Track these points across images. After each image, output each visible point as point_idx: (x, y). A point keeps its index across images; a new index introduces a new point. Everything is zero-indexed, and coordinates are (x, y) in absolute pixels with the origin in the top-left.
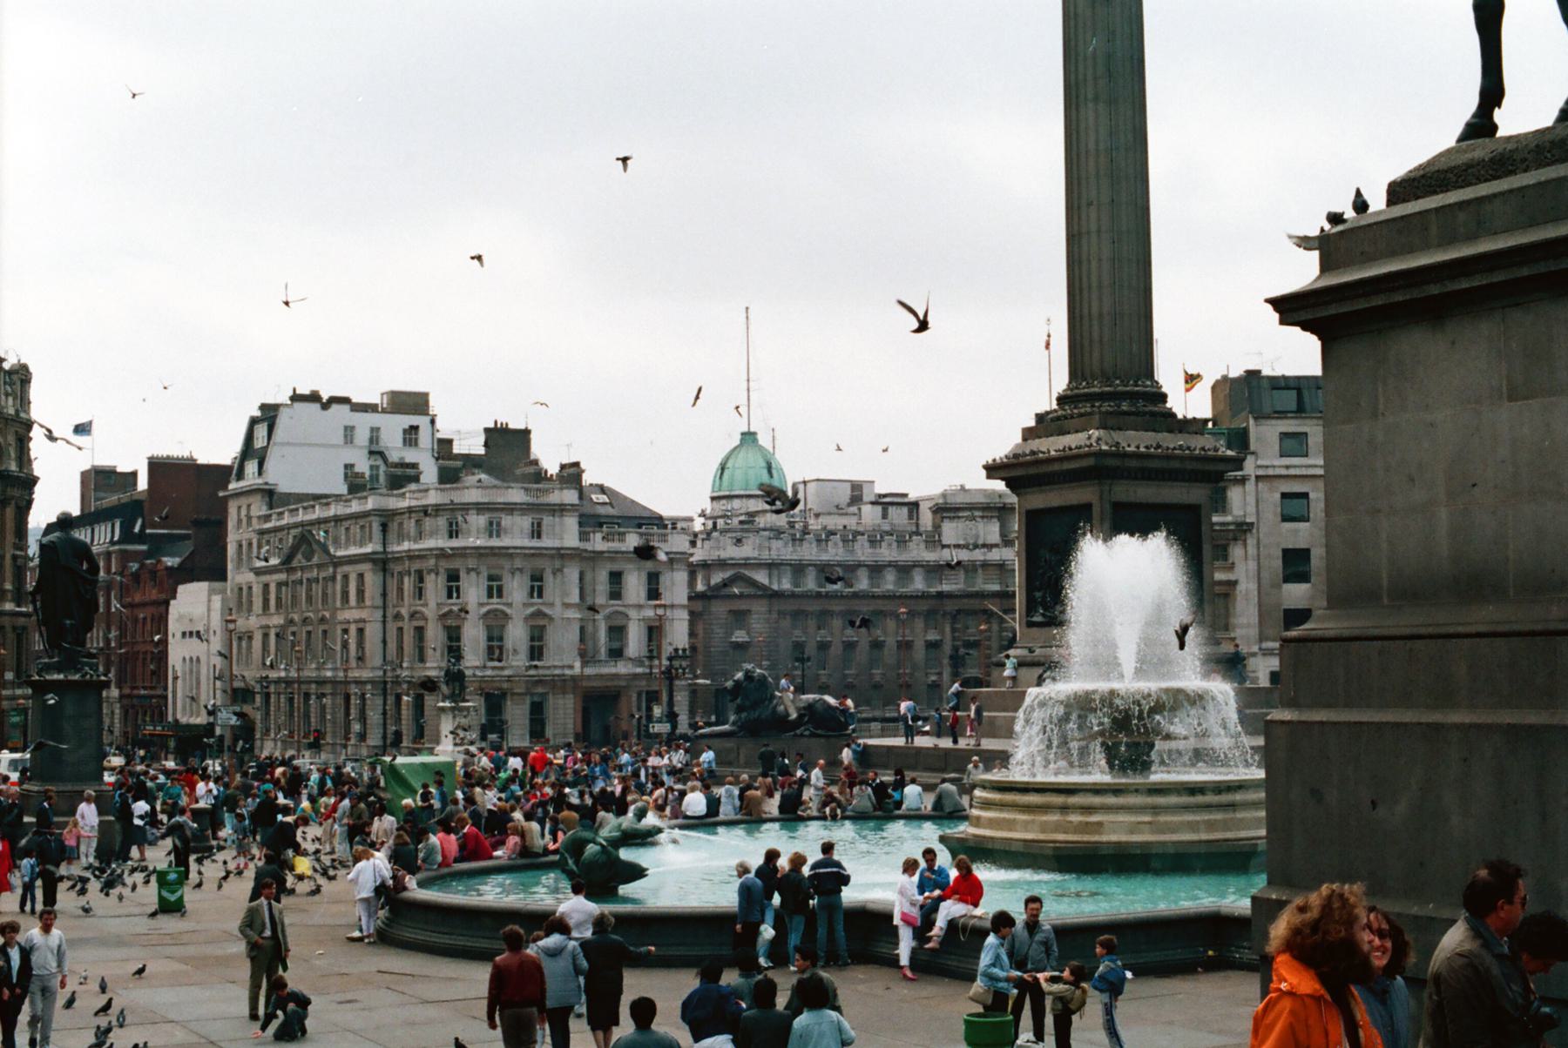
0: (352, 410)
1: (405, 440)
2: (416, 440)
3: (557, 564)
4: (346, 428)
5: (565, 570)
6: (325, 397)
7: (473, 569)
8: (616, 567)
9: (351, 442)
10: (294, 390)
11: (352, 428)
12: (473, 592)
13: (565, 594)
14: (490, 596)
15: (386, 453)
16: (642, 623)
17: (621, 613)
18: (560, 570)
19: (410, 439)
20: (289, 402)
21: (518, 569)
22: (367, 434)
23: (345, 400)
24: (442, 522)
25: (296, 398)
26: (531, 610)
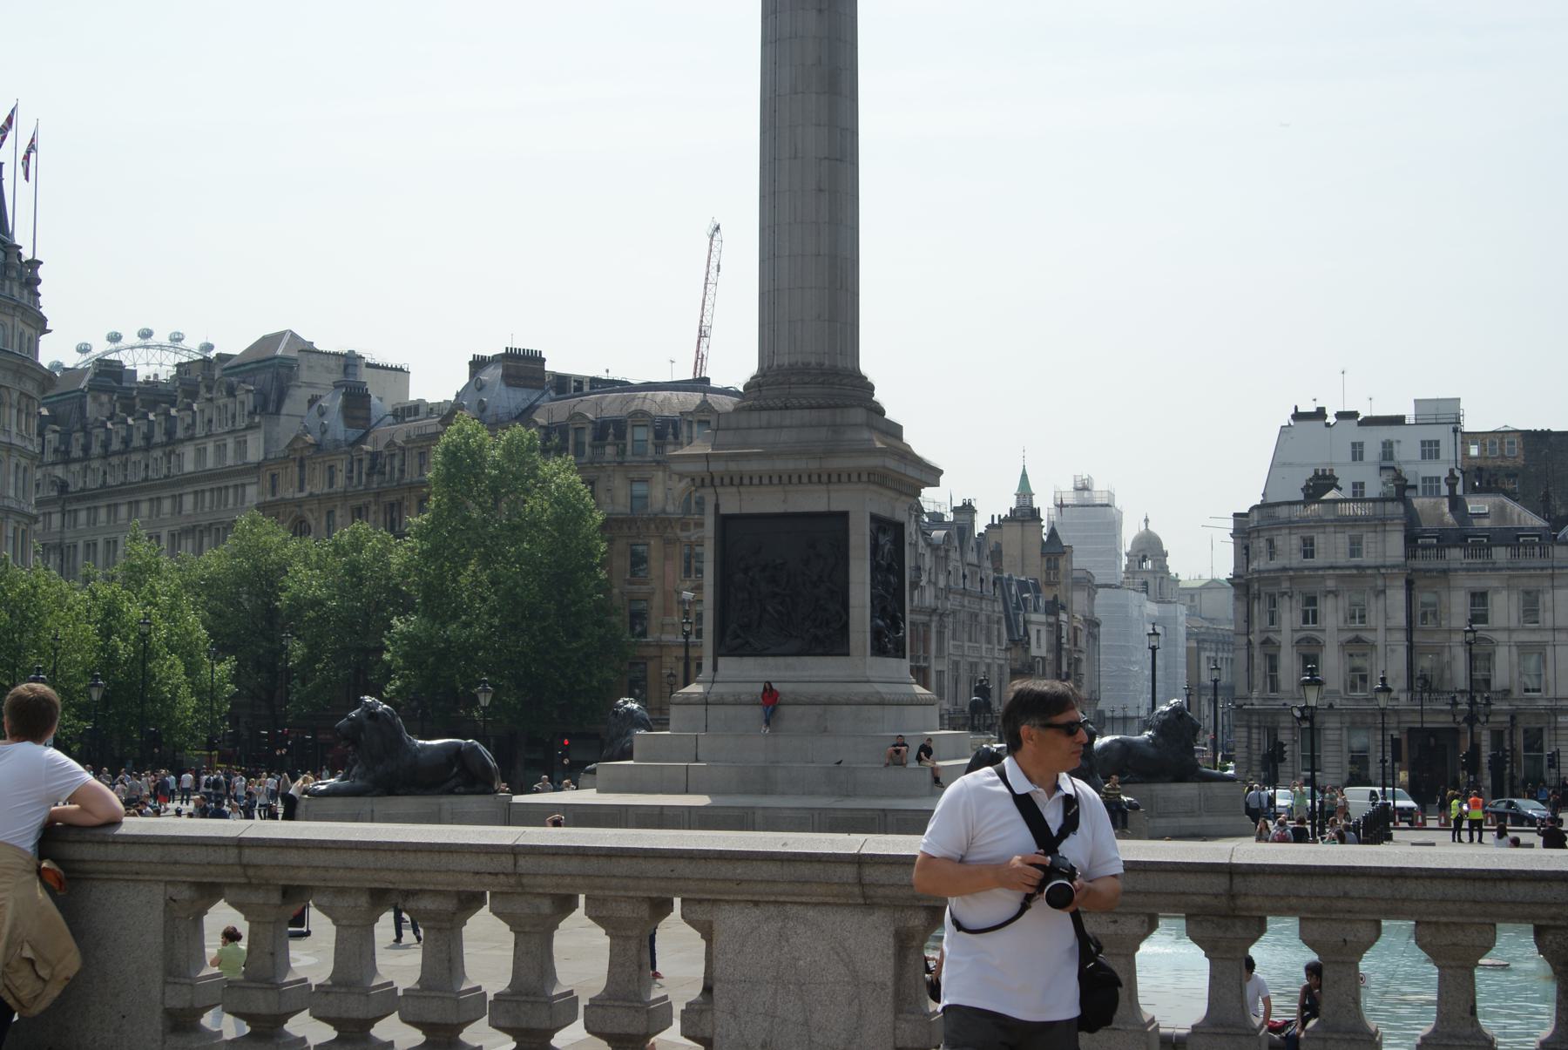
0: (1361, 424)
1: (1423, 452)
2: (1437, 452)
3: (1380, 582)
4: (1354, 445)
5: (1387, 591)
7: (1285, 593)
8: (1478, 584)
9: (1361, 459)
10: (1296, 408)
11: (1361, 444)
12: (1290, 617)
13: (1387, 617)
14: (1306, 621)
15: (1396, 467)
16: (1514, 650)
17: (1485, 639)
18: (1384, 592)
19: (1430, 451)
21: (1330, 592)
22: (1380, 449)
23: (1355, 415)
24: (1262, 543)
25: (1298, 416)
26: (1351, 635)
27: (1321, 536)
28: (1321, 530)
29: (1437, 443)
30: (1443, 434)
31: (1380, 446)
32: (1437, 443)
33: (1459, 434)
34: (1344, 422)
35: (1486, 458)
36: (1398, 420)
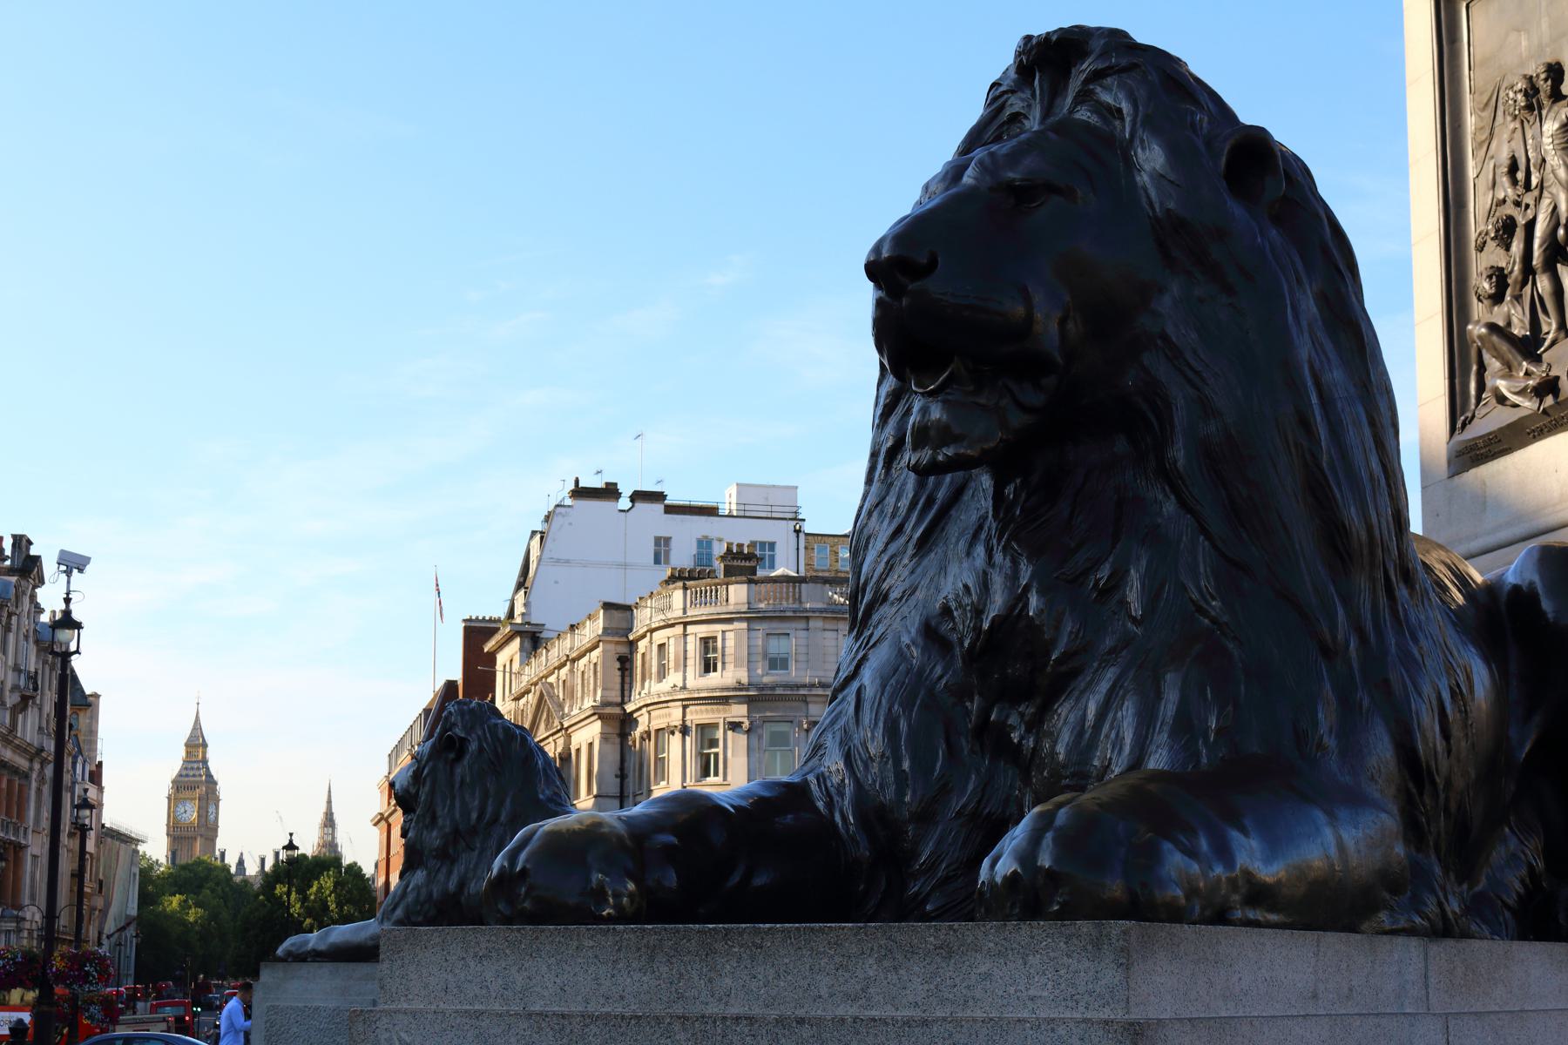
0: (672, 510)
4: (658, 540)
6: (626, 490)
10: (577, 481)
11: (667, 540)
20: (568, 502)
22: (694, 551)
23: (658, 497)
25: (580, 493)
27: (803, 634)
28: (802, 625)
29: (772, 545)
30: (780, 534)
31: (695, 545)
32: (772, 545)
33: (802, 536)
34: (639, 505)
35: (837, 571)
36: (710, 511)
